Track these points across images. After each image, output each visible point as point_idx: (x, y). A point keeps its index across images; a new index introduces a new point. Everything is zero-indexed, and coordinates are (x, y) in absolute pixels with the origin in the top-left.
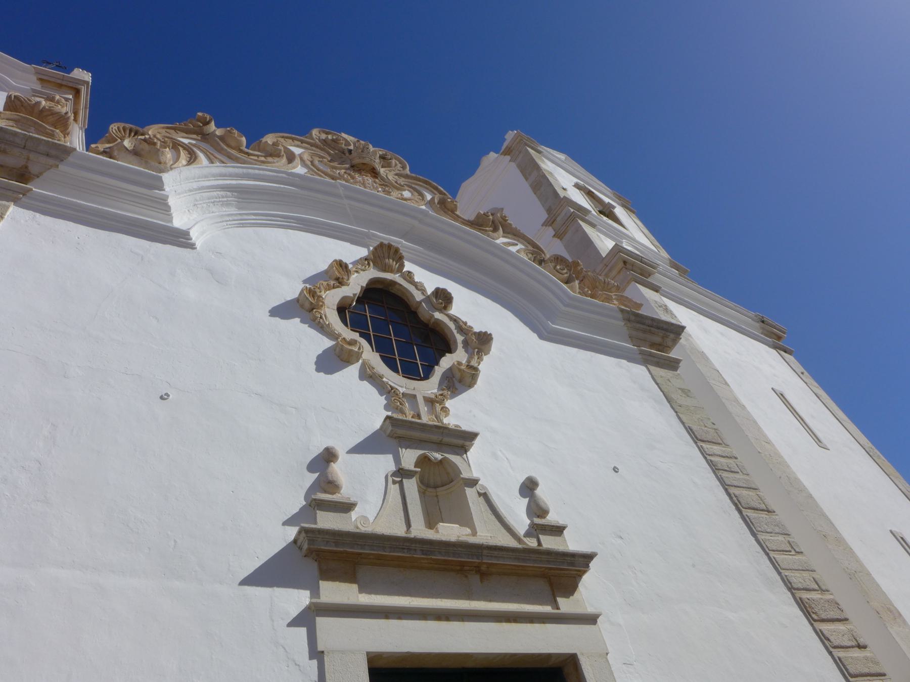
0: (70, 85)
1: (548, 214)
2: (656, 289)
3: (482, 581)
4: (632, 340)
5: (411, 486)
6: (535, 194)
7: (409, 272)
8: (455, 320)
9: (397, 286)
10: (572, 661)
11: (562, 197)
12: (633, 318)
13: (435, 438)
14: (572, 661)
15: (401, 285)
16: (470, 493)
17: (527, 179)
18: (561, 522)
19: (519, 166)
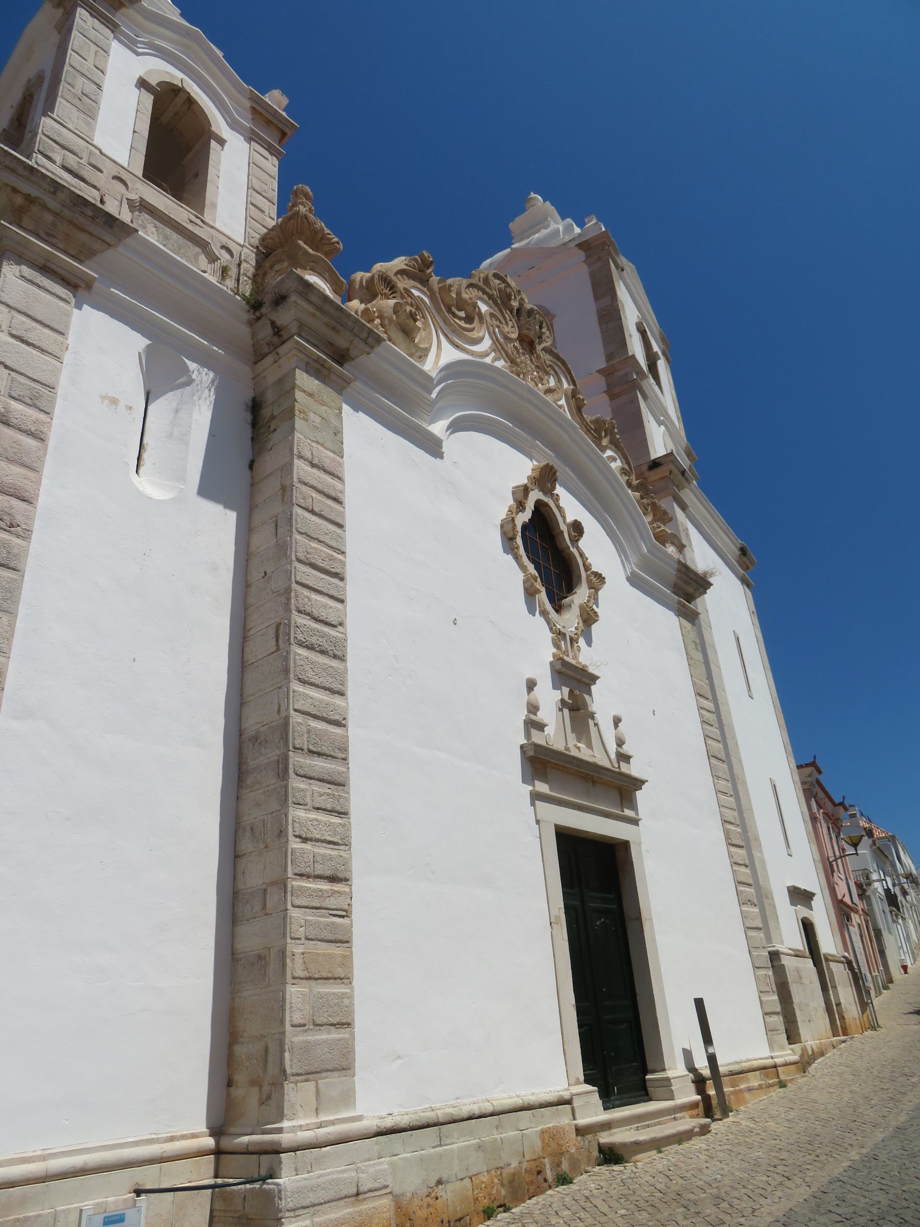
0: (280, 126)
1: (607, 361)
2: (684, 507)
3: (593, 786)
4: (674, 588)
5: (566, 711)
6: (600, 326)
7: (557, 495)
8: (582, 555)
9: (548, 508)
10: (626, 845)
11: (630, 354)
12: (684, 570)
13: (578, 677)
14: (626, 845)
15: (551, 509)
16: (591, 722)
17: (597, 298)
18: (630, 753)
19: (592, 275)
